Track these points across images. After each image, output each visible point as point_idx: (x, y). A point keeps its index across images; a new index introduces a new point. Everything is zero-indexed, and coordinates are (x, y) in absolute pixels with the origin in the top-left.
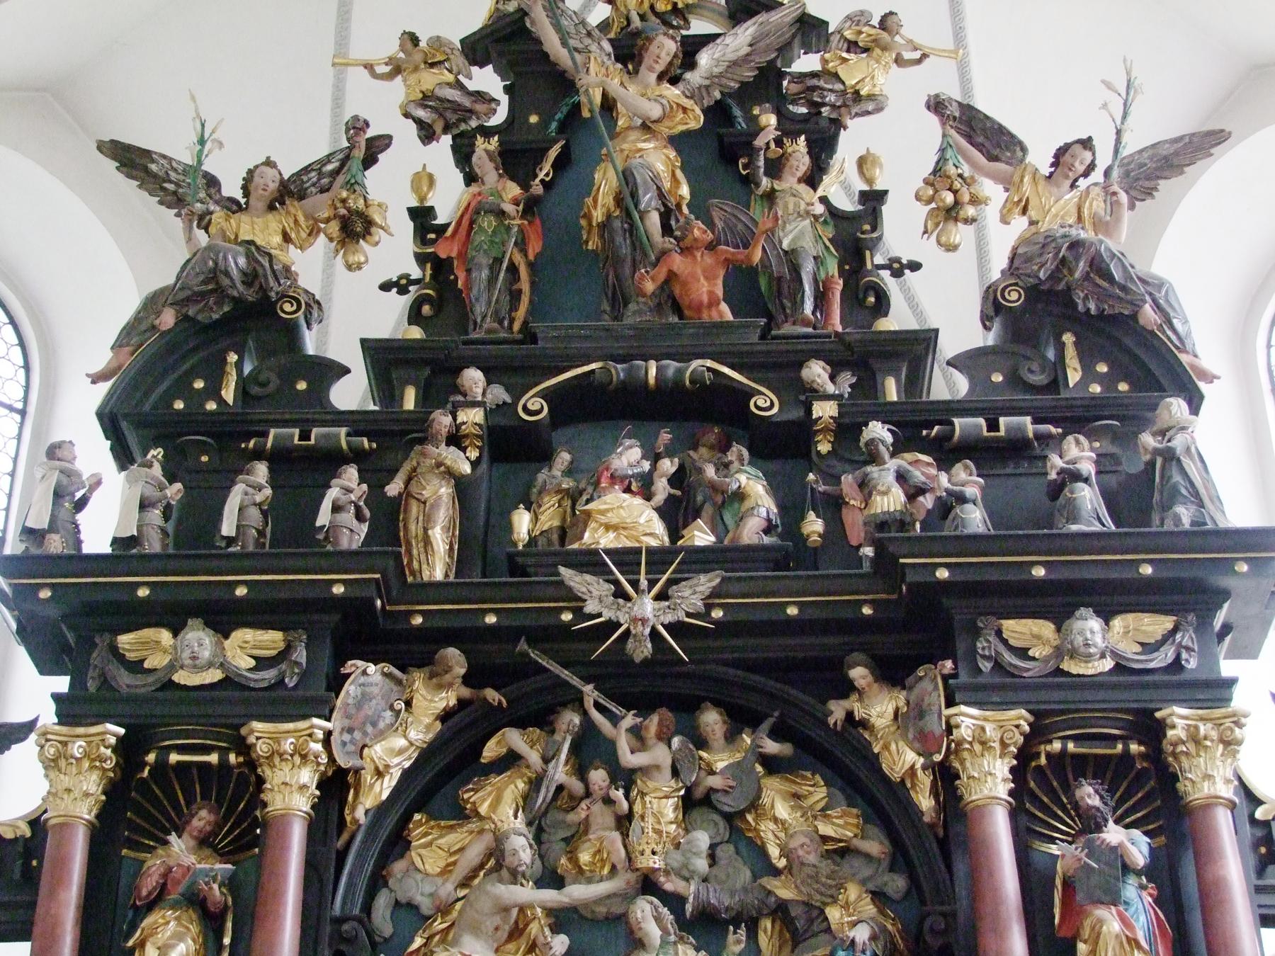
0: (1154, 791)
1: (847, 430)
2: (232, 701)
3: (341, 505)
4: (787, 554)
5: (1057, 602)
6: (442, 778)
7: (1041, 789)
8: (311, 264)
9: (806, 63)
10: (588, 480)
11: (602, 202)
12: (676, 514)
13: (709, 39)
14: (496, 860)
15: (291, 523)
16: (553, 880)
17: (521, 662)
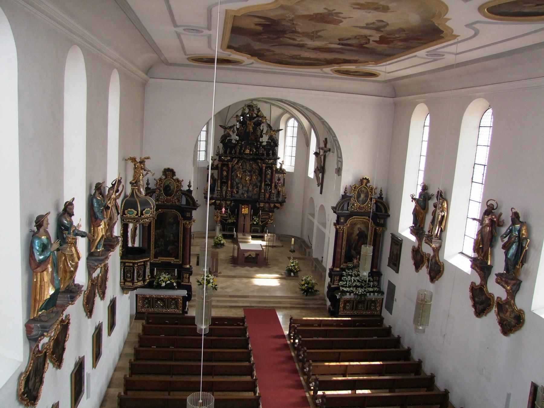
0: (271, 168)
1: (260, 147)
2: (228, 161)
3: (233, 152)
4: (256, 154)
5: (269, 160)
6: (237, 163)
7: (266, 168)
8: (231, 133)
9: (260, 119)
10: (246, 148)
11: (248, 131)
12: (250, 150)
13: (255, 118)
14: (239, 168)
15: (230, 153)
16: (242, 169)
17: (241, 157)
